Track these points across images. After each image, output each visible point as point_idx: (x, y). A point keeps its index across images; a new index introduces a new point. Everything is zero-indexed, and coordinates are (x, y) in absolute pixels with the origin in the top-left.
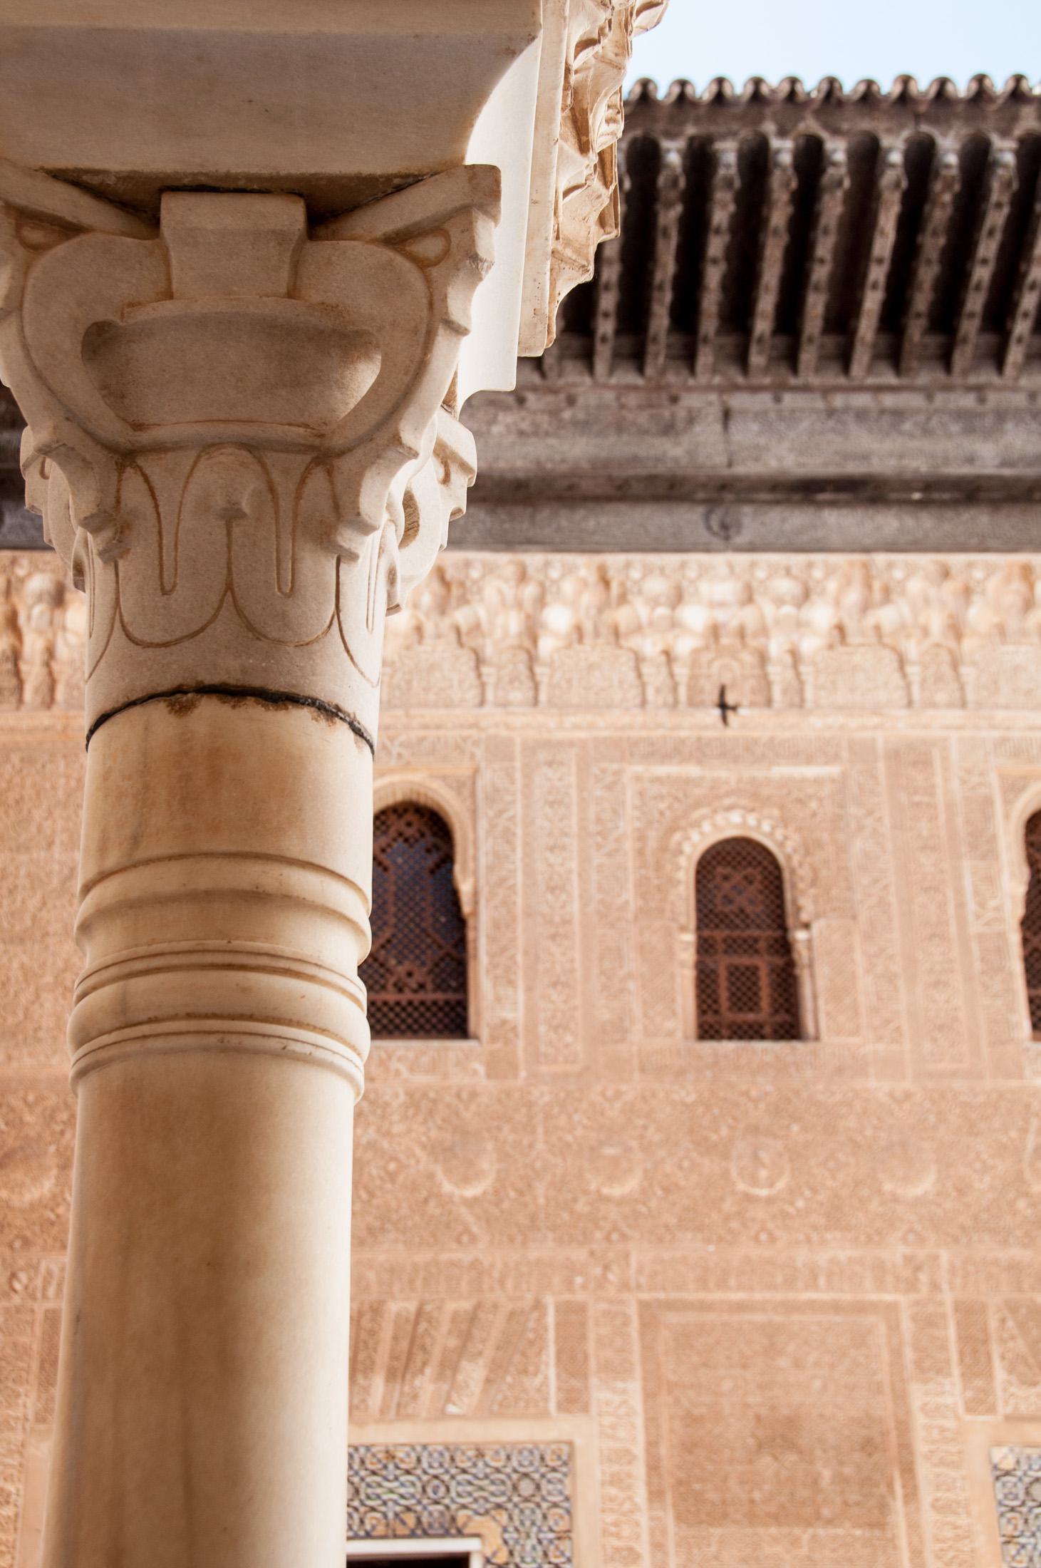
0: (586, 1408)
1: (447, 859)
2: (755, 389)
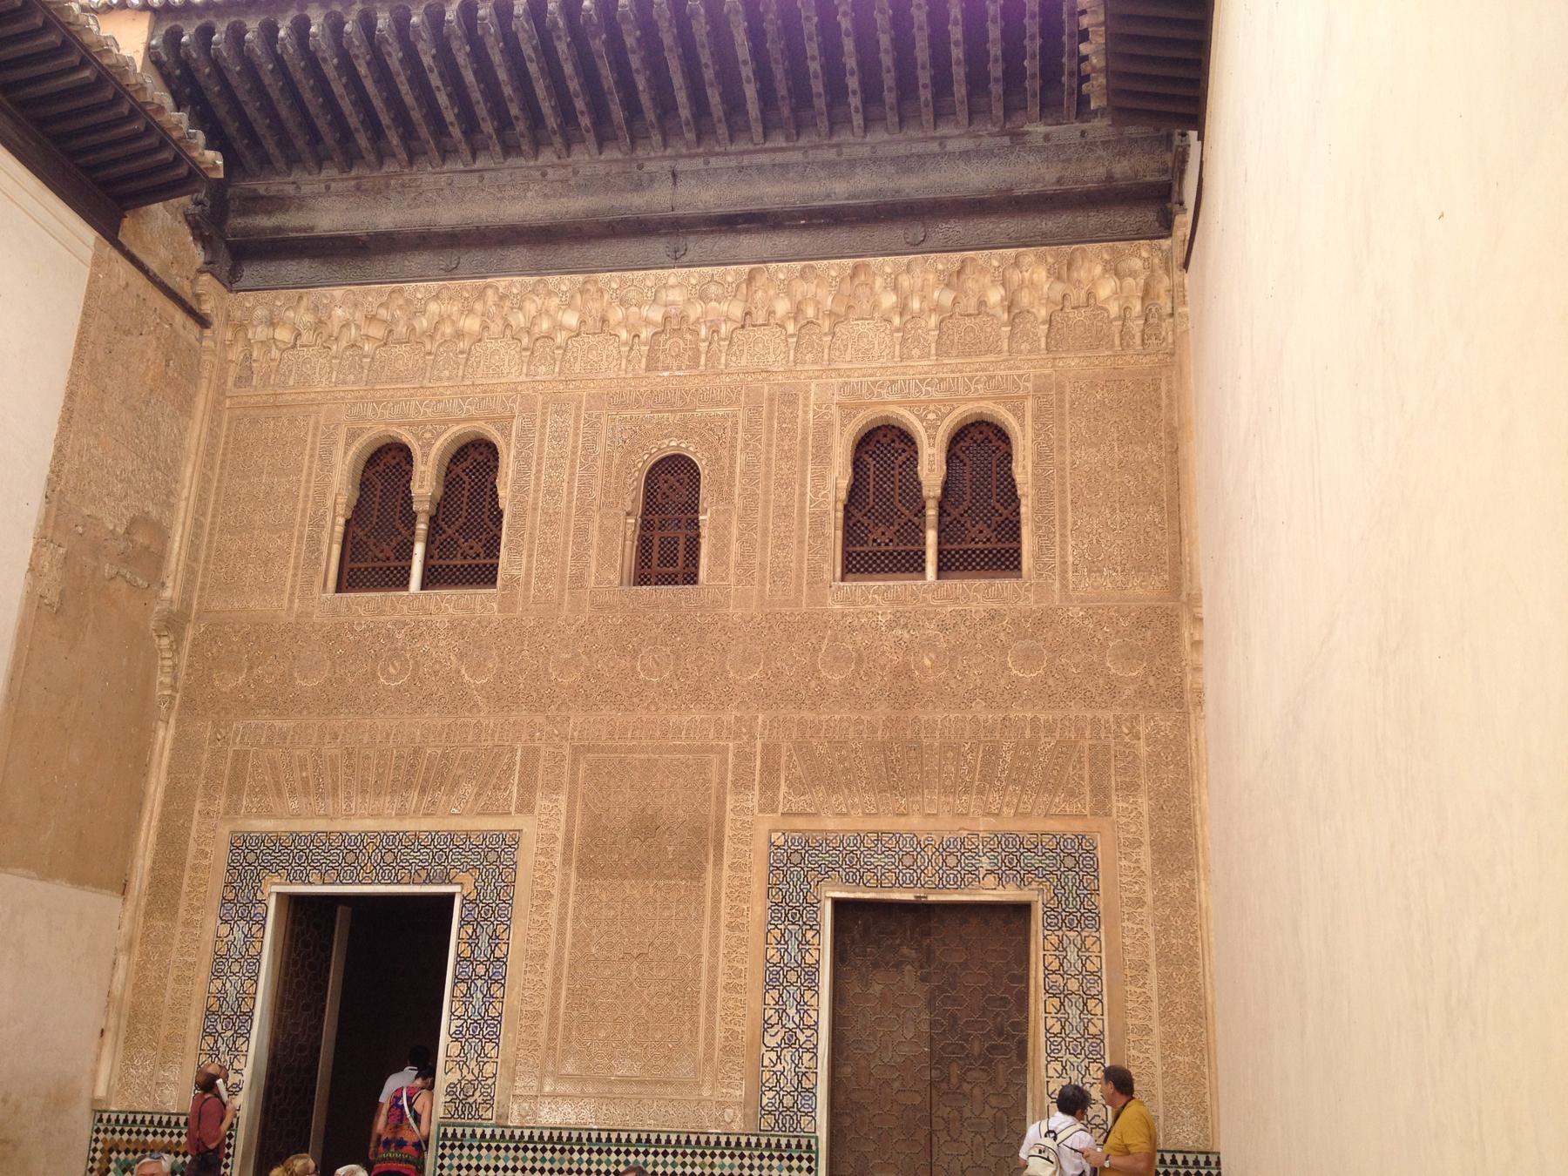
0: (531, 812)
2: (691, 156)
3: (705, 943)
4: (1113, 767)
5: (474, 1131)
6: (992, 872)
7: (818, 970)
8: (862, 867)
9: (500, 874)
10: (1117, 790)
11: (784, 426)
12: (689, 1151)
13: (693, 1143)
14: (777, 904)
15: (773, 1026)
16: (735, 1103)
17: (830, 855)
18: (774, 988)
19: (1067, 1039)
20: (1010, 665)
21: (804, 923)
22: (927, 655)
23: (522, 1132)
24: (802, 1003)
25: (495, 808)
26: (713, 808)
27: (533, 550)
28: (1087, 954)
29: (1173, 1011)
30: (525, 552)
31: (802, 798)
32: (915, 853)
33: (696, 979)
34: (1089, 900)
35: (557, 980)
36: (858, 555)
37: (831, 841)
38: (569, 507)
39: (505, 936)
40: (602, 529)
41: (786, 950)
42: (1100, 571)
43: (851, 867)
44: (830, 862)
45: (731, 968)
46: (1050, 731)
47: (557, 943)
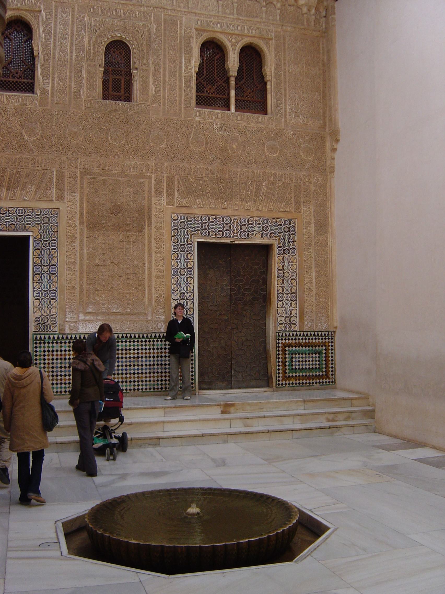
0: (63, 200)
1: (31, 38)
3: (146, 259)
4: (302, 194)
5: (49, 336)
6: (259, 232)
7: (193, 270)
8: (209, 229)
9: (51, 227)
10: (303, 203)
11: (172, 34)
12: (144, 340)
13: (145, 337)
14: (175, 243)
15: (175, 291)
16: (162, 321)
17: (197, 224)
18: (176, 277)
19: (285, 294)
20: (266, 151)
21: (187, 251)
22: (234, 144)
23: (71, 336)
24: (187, 282)
25: (45, 198)
26: (146, 202)
27: (54, 78)
28: (292, 263)
29: (319, 283)
30: (50, 78)
31: (184, 200)
32: (230, 224)
33: (144, 273)
34: (293, 244)
35: (81, 274)
36: (200, 97)
37: (197, 218)
38: (71, 59)
39: (55, 255)
40: (89, 72)
41: (180, 262)
42: (298, 116)
43: (205, 229)
44: (196, 227)
45: (158, 269)
46: (280, 179)
47: (80, 258)
